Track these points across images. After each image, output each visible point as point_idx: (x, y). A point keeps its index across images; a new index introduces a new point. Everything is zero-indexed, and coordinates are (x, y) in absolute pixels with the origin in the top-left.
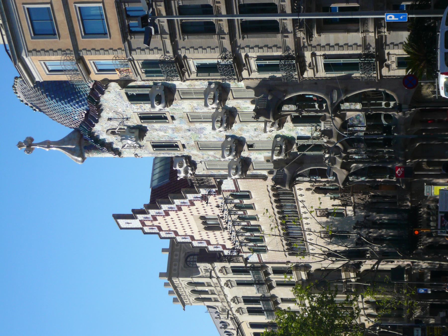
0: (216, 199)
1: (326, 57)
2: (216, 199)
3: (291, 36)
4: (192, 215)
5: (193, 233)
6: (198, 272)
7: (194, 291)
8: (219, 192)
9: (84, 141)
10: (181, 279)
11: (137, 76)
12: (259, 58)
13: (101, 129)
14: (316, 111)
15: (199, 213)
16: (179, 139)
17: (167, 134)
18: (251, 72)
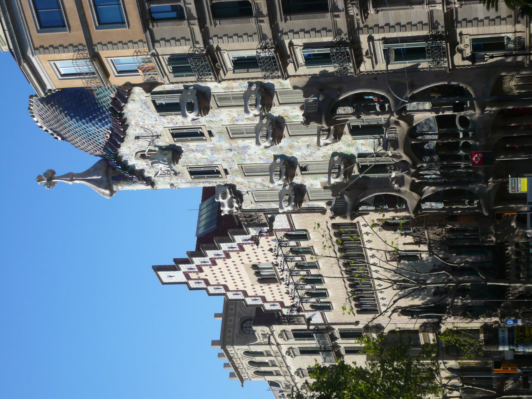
0: (268, 242)
1: (386, 41)
2: (268, 242)
3: (342, 14)
4: (242, 263)
5: (245, 287)
6: (255, 339)
7: (252, 363)
8: (271, 232)
9: (113, 170)
10: (236, 347)
11: (164, 77)
12: (306, 46)
13: (128, 151)
14: (377, 114)
15: (250, 261)
16: (220, 161)
17: (206, 157)
18: (298, 67)
